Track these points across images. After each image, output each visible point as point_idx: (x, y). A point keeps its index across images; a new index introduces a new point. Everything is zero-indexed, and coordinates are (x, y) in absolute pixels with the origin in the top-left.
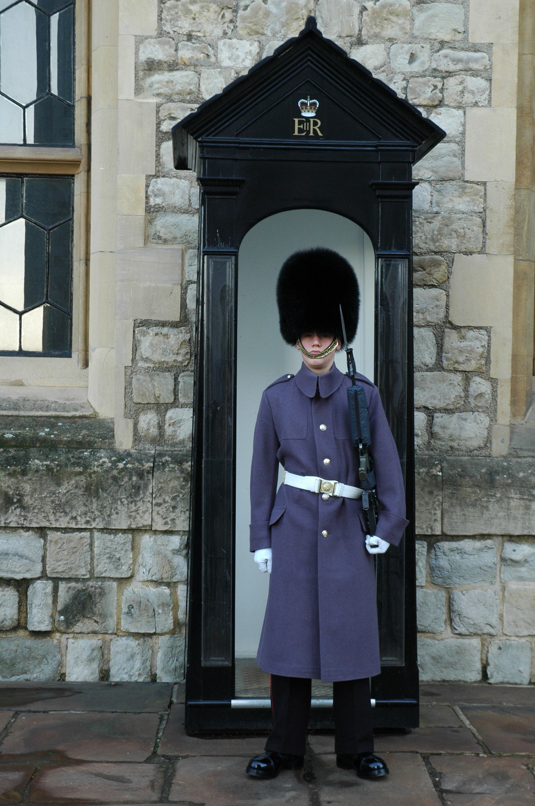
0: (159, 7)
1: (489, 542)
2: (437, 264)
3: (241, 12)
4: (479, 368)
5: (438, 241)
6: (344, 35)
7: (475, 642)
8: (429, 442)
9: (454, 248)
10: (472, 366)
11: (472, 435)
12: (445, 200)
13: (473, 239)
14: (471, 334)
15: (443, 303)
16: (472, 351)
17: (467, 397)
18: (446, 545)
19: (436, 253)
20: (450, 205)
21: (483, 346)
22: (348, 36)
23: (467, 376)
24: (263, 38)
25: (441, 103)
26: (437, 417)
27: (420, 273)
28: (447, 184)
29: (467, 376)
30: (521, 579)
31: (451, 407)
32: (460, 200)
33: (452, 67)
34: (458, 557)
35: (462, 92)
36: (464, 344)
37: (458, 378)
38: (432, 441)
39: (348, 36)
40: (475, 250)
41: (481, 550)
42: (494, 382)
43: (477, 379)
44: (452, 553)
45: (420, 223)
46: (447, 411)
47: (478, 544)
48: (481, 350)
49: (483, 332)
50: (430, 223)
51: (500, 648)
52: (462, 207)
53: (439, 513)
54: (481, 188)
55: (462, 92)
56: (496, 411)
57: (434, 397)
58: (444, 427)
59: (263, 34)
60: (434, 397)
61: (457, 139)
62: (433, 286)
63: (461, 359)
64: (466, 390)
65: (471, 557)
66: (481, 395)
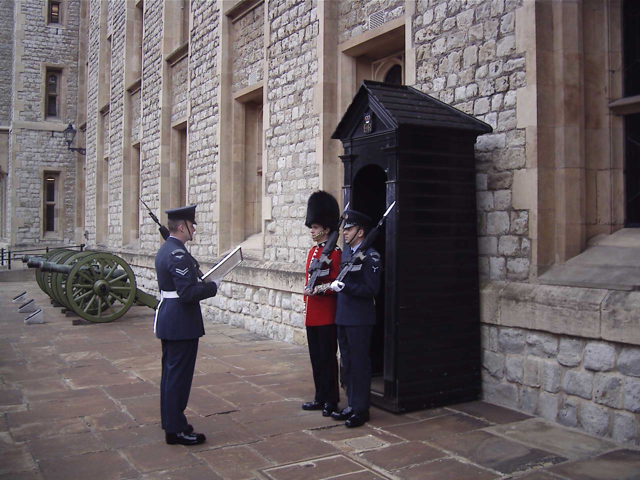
0: (416, 70)
1: (520, 332)
2: (507, 176)
3: (440, 65)
4: (525, 233)
5: (507, 164)
6: (472, 64)
7: (514, 386)
8: (507, 275)
9: (514, 167)
10: (520, 232)
11: (522, 271)
12: (510, 141)
13: (521, 161)
14: (522, 214)
15: (509, 198)
16: (521, 223)
17: (520, 249)
18: (503, 331)
19: (507, 170)
20: (512, 144)
21: (526, 220)
22: (473, 65)
23: (521, 237)
24: (447, 74)
25: (508, 89)
26: (508, 261)
27: (501, 182)
28: (511, 132)
29: (521, 237)
30: (534, 354)
31: (514, 255)
32: (516, 140)
33: (511, 69)
34: (507, 338)
35: (516, 81)
36: (518, 220)
37: (516, 238)
38: (508, 273)
39: (473, 65)
40: (521, 167)
41: (517, 335)
42: (530, 240)
43: (525, 239)
44: (505, 336)
45: (501, 155)
46: (514, 257)
47: (516, 332)
48: (524, 223)
49: (526, 212)
50: (505, 154)
51: (524, 392)
52: (517, 144)
53: (499, 312)
54: (524, 131)
55: (516, 81)
56: (531, 257)
57: (506, 249)
58: (510, 266)
59: (447, 73)
60: (506, 249)
61: (515, 107)
62: (506, 189)
63: (517, 228)
64: (520, 246)
65: (513, 339)
66: (525, 248)
